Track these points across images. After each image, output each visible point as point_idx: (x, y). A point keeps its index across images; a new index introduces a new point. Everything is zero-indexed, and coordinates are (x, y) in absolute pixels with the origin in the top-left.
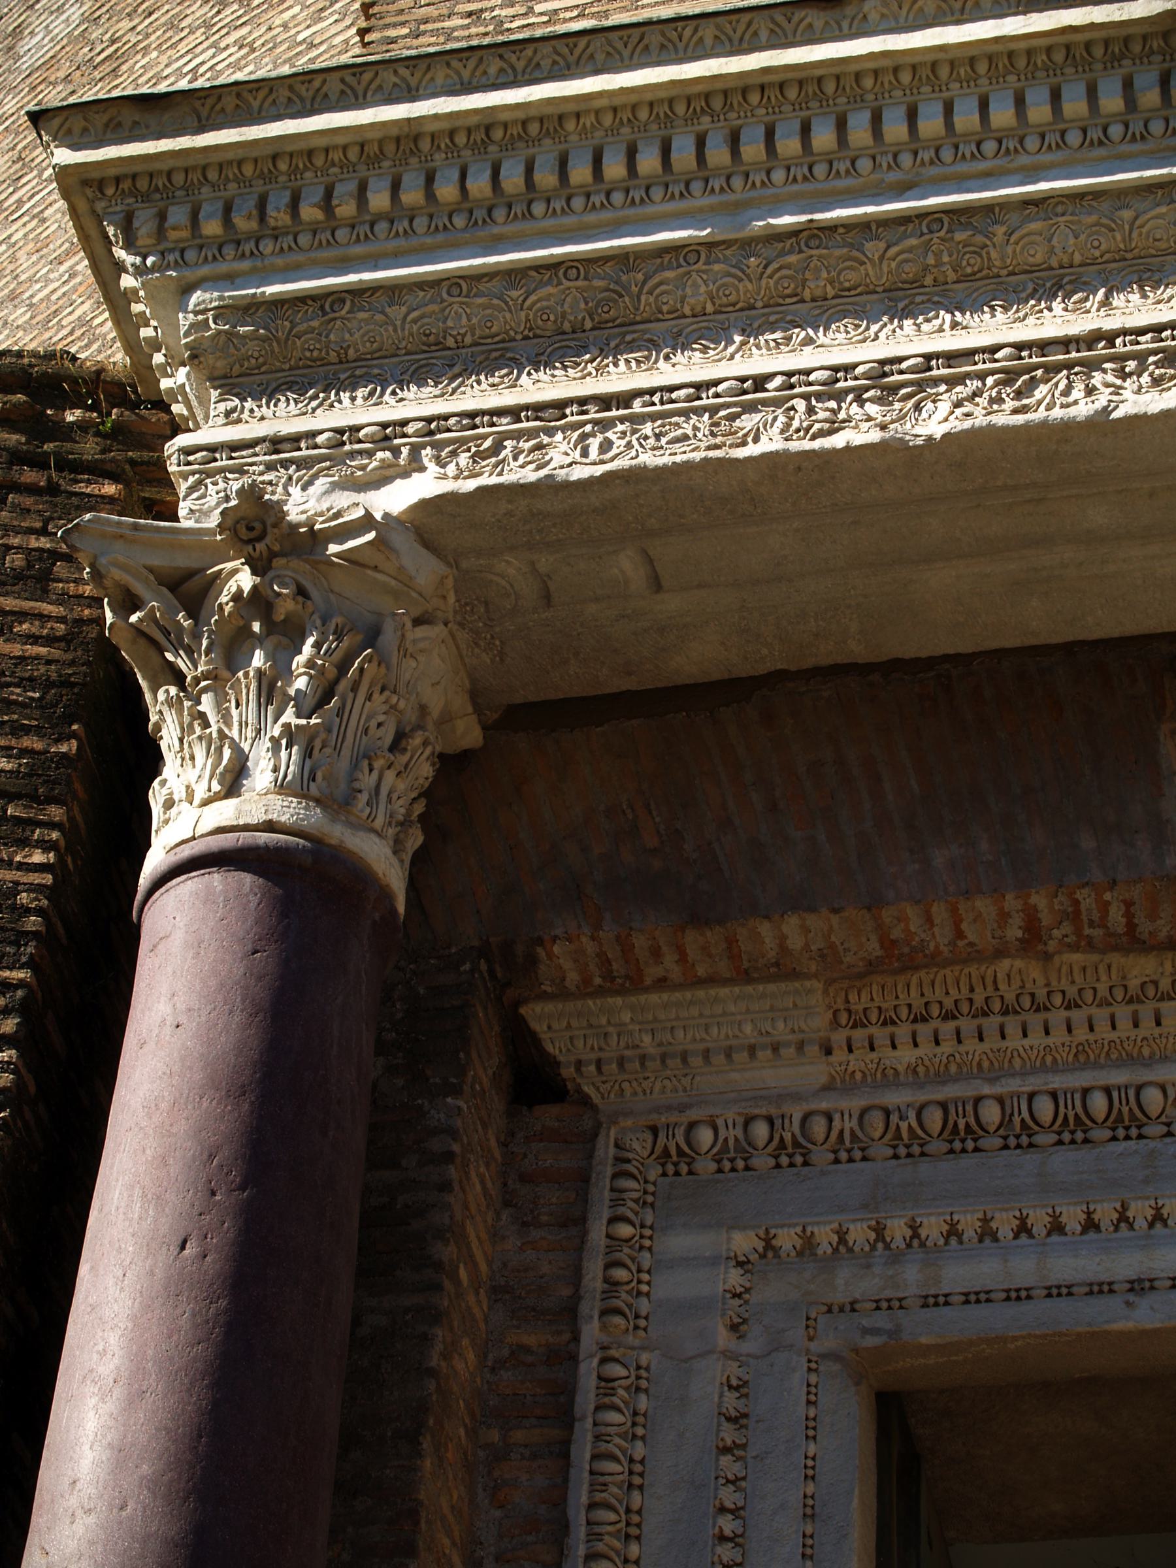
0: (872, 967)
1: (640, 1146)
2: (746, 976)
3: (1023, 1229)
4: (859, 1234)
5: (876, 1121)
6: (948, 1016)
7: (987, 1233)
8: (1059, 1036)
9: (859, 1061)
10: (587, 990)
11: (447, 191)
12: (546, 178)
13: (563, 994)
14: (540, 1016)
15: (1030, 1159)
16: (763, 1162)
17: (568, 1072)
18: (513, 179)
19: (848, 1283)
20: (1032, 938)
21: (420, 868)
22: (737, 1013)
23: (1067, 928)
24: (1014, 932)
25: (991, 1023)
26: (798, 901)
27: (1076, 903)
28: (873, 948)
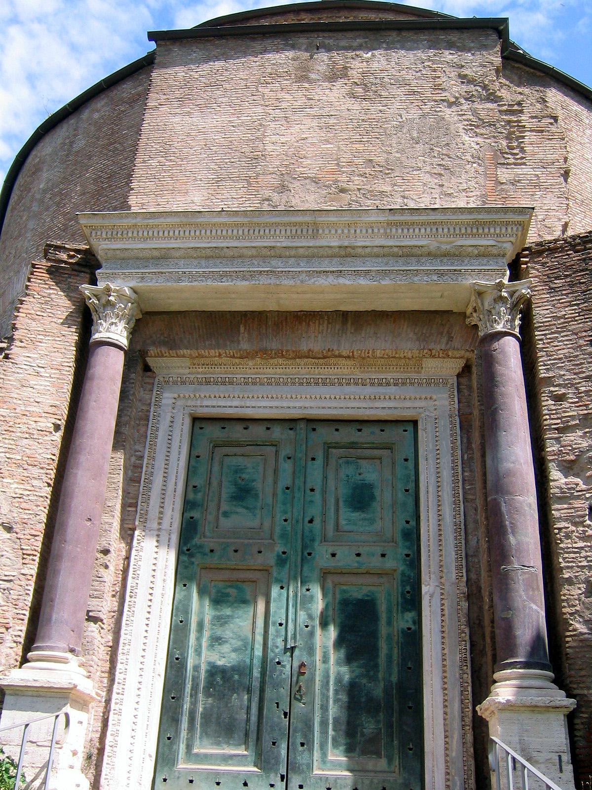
0: (197, 357)
1: (162, 379)
3: (215, 397)
4: (192, 396)
5: (196, 379)
7: (210, 397)
8: (223, 369)
9: (194, 370)
11: (140, 234)
12: (156, 234)
13: (152, 357)
14: (148, 359)
16: (179, 384)
18: (151, 233)
19: (190, 403)
20: (220, 355)
21: (131, 342)
22: (176, 361)
28: (197, 355)
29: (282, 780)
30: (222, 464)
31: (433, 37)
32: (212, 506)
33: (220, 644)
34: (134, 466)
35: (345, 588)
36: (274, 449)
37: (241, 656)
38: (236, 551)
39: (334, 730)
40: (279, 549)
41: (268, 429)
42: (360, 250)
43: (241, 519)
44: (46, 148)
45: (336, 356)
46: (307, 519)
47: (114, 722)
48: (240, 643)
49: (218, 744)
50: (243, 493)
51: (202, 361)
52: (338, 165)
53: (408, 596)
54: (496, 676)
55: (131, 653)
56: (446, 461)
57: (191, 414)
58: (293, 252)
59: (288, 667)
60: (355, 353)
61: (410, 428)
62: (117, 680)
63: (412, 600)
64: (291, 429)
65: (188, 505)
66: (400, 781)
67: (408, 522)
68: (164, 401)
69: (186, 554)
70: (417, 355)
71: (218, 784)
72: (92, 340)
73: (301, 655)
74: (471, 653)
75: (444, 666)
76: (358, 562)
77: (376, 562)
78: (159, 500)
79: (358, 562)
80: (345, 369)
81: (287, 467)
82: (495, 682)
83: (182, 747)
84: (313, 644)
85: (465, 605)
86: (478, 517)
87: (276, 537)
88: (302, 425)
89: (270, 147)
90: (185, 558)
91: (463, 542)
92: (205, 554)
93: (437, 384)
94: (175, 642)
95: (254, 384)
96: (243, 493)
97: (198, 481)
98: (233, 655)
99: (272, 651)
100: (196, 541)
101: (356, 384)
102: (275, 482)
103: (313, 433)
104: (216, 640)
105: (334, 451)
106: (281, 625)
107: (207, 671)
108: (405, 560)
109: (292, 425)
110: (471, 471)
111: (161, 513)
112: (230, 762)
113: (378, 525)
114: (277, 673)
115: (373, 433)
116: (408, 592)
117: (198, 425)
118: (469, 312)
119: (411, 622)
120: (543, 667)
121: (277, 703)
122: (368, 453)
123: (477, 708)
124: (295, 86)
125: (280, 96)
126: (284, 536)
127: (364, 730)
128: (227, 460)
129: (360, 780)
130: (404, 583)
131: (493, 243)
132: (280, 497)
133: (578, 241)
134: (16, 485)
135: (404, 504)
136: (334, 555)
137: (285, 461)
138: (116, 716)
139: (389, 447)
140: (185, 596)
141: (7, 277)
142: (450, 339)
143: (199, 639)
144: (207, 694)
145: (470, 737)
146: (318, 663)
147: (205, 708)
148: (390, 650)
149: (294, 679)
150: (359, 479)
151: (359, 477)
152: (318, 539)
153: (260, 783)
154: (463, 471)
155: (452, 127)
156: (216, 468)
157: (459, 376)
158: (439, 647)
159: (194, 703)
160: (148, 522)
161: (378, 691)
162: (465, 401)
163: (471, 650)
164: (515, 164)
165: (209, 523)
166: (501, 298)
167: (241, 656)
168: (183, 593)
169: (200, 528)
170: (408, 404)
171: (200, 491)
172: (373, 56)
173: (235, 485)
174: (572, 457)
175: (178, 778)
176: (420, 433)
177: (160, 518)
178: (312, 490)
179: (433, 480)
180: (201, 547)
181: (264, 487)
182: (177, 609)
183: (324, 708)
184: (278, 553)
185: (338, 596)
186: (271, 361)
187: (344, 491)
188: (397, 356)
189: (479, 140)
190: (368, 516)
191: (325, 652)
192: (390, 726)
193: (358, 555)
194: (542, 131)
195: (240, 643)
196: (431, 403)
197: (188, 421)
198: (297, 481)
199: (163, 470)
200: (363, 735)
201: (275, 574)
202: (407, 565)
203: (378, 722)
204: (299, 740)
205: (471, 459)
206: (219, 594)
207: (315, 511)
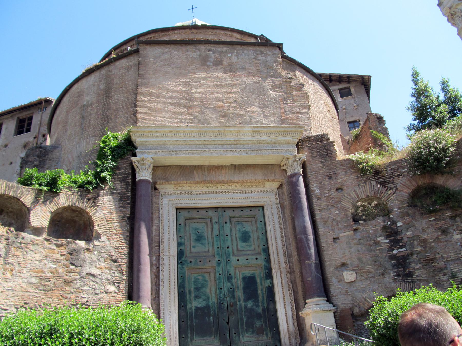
18: (158, 135)
19: (175, 202)
20: (186, 183)
21: (152, 179)
22: (168, 186)
26: (173, 181)
30: (189, 226)
31: (254, 49)
32: (188, 244)
35: (243, 272)
36: (210, 219)
38: (200, 261)
40: (217, 259)
41: (207, 212)
42: (242, 142)
43: (199, 248)
44: (84, 83)
45: (232, 182)
46: (226, 247)
48: (206, 297)
50: (199, 238)
51: (179, 185)
52: (223, 102)
53: (267, 274)
54: (307, 301)
56: (277, 221)
58: (216, 143)
59: (226, 305)
61: (261, 209)
63: (269, 275)
65: (179, 244)
66: (272, 343)
67: (264, 246)
68: (164, 202)
72: (137, 180)
73: (230, 300)
75: (284, 299)
77: (255, 262)
80: (235, 187)
81: (216, 227)
82: (306, 303)
83: (189, 340)
85: (289, 275)
87: (215, 255)
88: (220, 210)
89: (194, 94)
90: (180, 266)
95: (200, 194)
96: (199, 238)
97: (182, 234)
98: (204, 302)
100: (184, 259)
101: (240, 193)
102: (212, 233)
103: (224, 213)
104: (197, 297)
105: (233, 219)
106: (221, 289)
109: (216, 210)
111: (169, 248)
113: (252, 248)
115: (247, 212)
117: (178, 211)
118: (282, 165)
120: (324, 297)
122: (246, 219)
123: (300, 313)
124: (202, 68)
125: (195, 71)
126: (218, 254)
128: (191, 225)
130: (265, 269)
131: (291, 139)
132: (215, 238)
133: (319, 137)
134: (115, 243)
135: (262, 239)
136: (238, 260)
141: (71, 144)
142: (275, 175)
143: (190, 297)
145: (296, 324)
148: (263, 294)
151: (243, 229)
155: (265, 88)
156: (187, 228)
157: (278, 188)
158: (281, 292)
159: (192, 322)
161: (260, 310)
164: (290, 103)
166: (296, 160)
168: (182, 280)
169: (185, 253)
170: (260, 200)
172: (232, 55)
174: (326, 220)
176: (266, 211)
177: (169, 251)
178: (227, 235)
179: (272, 229)
180: (186, 261)
181: (208, 235)
182: (180, 286)
183: (242, 319)
185: (241, 276)
186: (207, 185)
187: (239, 235)
189: (277, 93)
190: (249, 244)
192: (266, 323)
193: (247, 259)
194: (299, 90)
195: (206, 297)
196: (268, 199)
198: (221, 232)
200: (256, 327)
201: (217, 269)
203: (261, 322)
204: (234, 332)
205: (285, 220)
207: (229, 243)
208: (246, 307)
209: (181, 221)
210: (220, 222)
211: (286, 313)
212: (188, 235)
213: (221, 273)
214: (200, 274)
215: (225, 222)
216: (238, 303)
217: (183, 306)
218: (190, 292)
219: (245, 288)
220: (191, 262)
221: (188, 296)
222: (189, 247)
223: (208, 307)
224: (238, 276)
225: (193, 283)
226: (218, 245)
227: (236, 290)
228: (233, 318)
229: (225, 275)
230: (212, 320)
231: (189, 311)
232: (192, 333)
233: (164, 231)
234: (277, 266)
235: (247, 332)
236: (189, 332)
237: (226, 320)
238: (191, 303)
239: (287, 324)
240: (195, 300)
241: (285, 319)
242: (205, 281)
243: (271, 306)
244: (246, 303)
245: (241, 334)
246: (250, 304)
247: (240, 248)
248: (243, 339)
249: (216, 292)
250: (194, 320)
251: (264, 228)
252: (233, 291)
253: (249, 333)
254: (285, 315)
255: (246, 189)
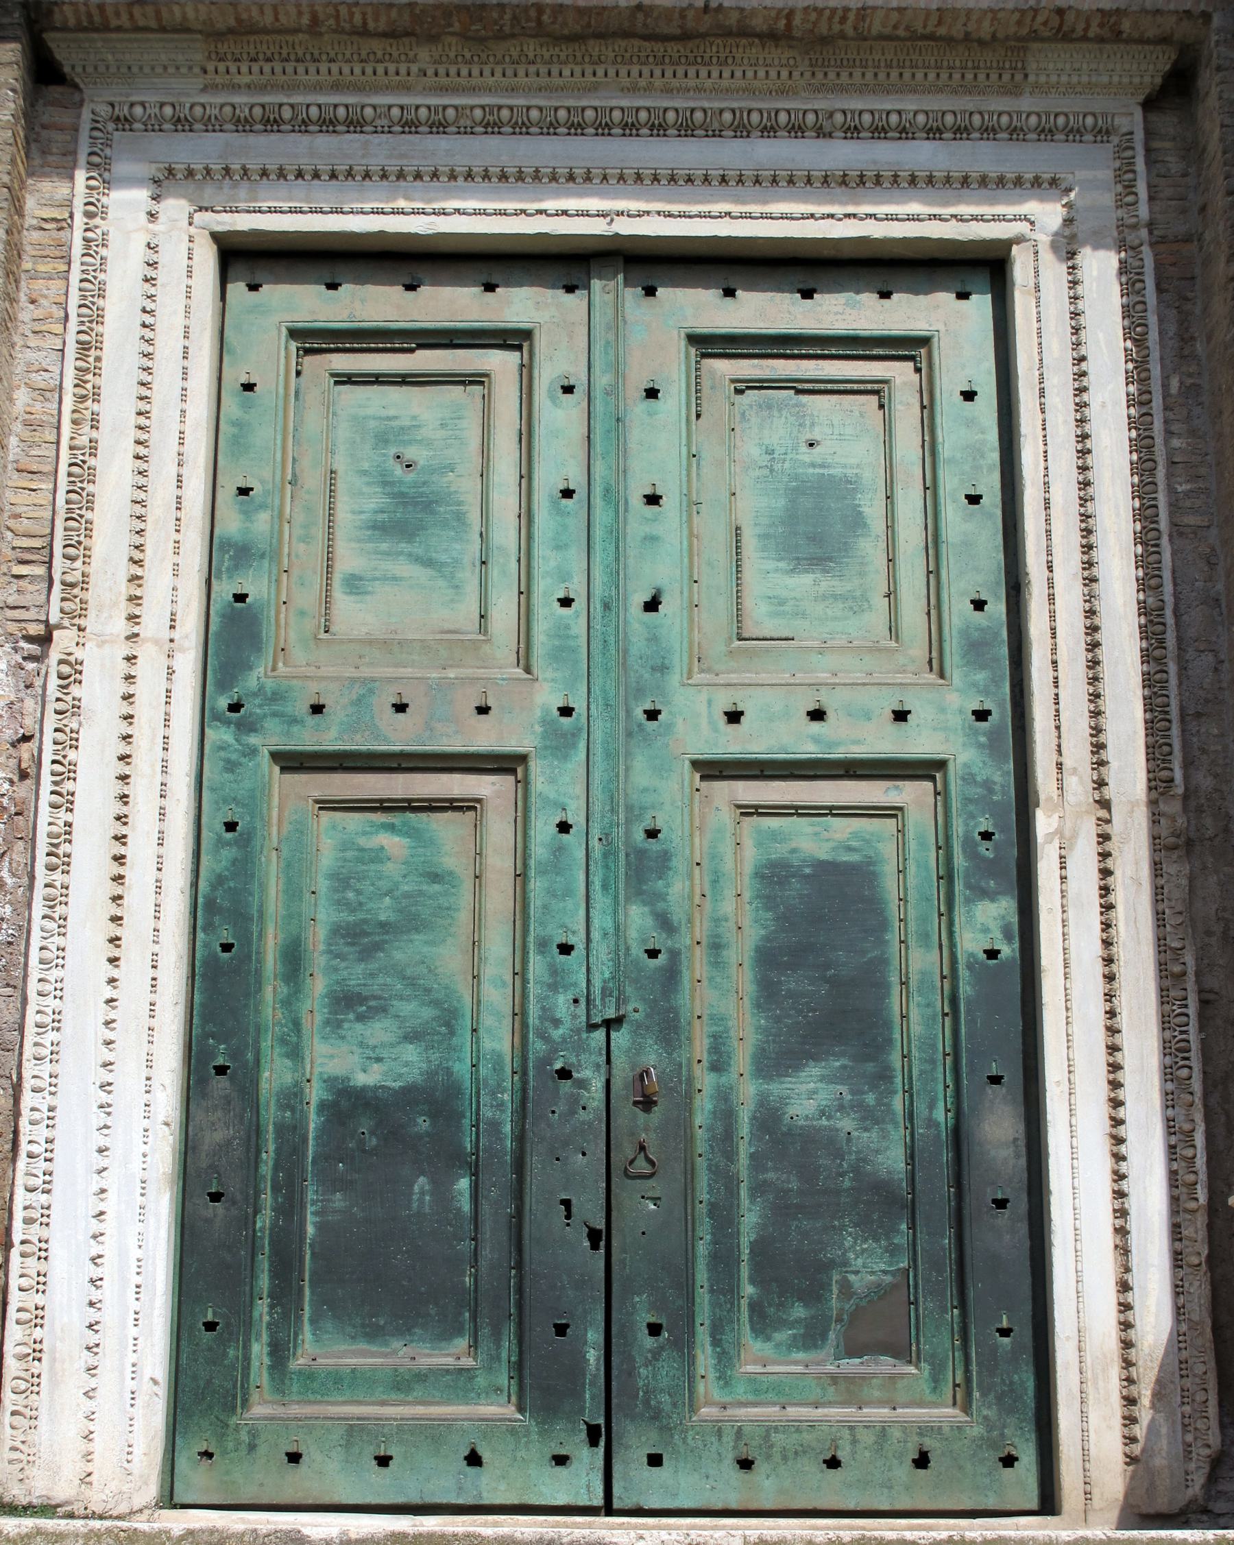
1: (103, 110)
2: (163, 29)
6: (268, 60)
10: (80, 29)
13: (64, 29)
15: (305, 139)
17: (67, 69)
23: (332, 22)
24: (305, 20)
25: (289, 68)
27: (338, 11)
29: (593, 1442)
33: (361, 1018)
34: (27, 424)
36: (513, 358)
37: (435, 1056)
38: (401, 708)
39: (752, 1281)
40: (548, 697)
45: (728, 33)
47: (24, 1282)
48: (427, 1013)
49: (373, 1333)
55: (65, 1054)
57: (216, 237)
59: (597, 1085)
60: (797, 21)
62: (24, 1147)
64: (570, 289)
65: (223, 554)
66: (977, 1430)
67: (979, 605)
69: (228, 723)
70: (1012, 30)
71: (383, 1461)
73: (637, 1050)
74: (1202, 1028)
75: (1115, 1067)
76: (816, 740)
77: (882, 742)
78: (127, 539)
79: (816, 740)
81: (560, 420)
83: (259, 1350)
84: (675, 1010)
85: (1176, 869)
86: (1220, 586)
90: (219, 735)
91: (1172, 668)
92: (294, 721)
93: (1074, 133)
94: (207, 1017)
96: (411, 513)
98: (411, 1053)
99: (543, 1036)
100: (257, 677)
102: (526, 476)
104: (349, 1004)
106: (566, 949)
107: (323, 1106)
108: (976, 732)
110: (1193, 433)
112: (418, 1393)
114: (561, 1108)
116: (986, 836)
119: (998, 935)
121: (567, 1203)
126: (560, 654)
127: (852, 1277)
129: (846, 1434)
136: (734, 717)
137: (553, 399)
138: (32, 1262)
139: (909, 347)
140: (234, 862)
143: (287, 1003)
144: (331, 1184)
145: (1199, 1289)
146: (698, 1070)
147: (320, 1227)
149: (619, 1122)
150: (807, 459)
152: (678, 662)
153: (522, 1453)
154: (1169, 433)
157: (1149, 105)
159: (290, 1208)
160: (92, 613)
162: (1169, 192)
163: (1201, 1017)
165: (302, 613)
167: (435, 1056)
168: (228, 854)
171: (262, 506)
173: (385, 484)
175: (252, 1447)
178: (653, 500)
180: (277, 697)
182: (211, 905)
184: (546, 711)
185: (751, 855)
188: (942, 31)
190: (840, 586)
191: (715, 1037)
195: (427, 1013)
197: (207, 259)
198: (599, 468)
199: (134, 434)
201: (539, 783)
202: (980, 746)
203: (893, 1251)
204: (646, 1317)
206: (349, 854)
208: (769, 1119)
209: (266, 355)
210: (603, 380)
211: (1120, 1194)
212: (313, 480)
213: (576, 817)
214: (396, 819)
215: (637, 381)
216: (706, 1081)
217: (221, 1070)
218: (294, 961)
219: (769, 960)
220: (317, 709)
221: (271, 992)
222: (317, 582)
223: (437, 1099)
224: (727, 849)
225: (323, 885)
226: (564, 576)
227: (697, 965)
228: (641, 1208)
229: (604, 839)
230: (466, 1207)
231: (270, 1115)
232: (285, 1295)
233: (104, 436)
234: (1079, 787)
235: (763, 1323)
236: (264, 1282)
237: (590, 1210)
238: (295, 1053)
239: (1124, 1287)
240: (334, 1025)
241: (1108, 1239)
242: (435, 877)
243: (998, 1128)
244: (776, 1088)
245: (703, 1335)
246: (809, 1095)
247: (761, 618)
248: (725, 1379)
249: (520, 974)
250: (310, 1196)
251: (995, 456)
252: (671, 976)
253: (782, 1336)
254: (1105, 1204)
255: (856, 104)
